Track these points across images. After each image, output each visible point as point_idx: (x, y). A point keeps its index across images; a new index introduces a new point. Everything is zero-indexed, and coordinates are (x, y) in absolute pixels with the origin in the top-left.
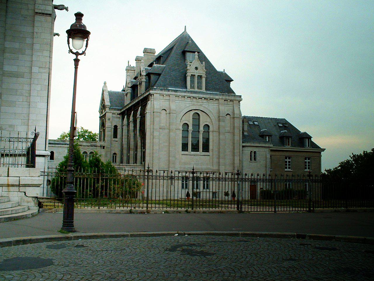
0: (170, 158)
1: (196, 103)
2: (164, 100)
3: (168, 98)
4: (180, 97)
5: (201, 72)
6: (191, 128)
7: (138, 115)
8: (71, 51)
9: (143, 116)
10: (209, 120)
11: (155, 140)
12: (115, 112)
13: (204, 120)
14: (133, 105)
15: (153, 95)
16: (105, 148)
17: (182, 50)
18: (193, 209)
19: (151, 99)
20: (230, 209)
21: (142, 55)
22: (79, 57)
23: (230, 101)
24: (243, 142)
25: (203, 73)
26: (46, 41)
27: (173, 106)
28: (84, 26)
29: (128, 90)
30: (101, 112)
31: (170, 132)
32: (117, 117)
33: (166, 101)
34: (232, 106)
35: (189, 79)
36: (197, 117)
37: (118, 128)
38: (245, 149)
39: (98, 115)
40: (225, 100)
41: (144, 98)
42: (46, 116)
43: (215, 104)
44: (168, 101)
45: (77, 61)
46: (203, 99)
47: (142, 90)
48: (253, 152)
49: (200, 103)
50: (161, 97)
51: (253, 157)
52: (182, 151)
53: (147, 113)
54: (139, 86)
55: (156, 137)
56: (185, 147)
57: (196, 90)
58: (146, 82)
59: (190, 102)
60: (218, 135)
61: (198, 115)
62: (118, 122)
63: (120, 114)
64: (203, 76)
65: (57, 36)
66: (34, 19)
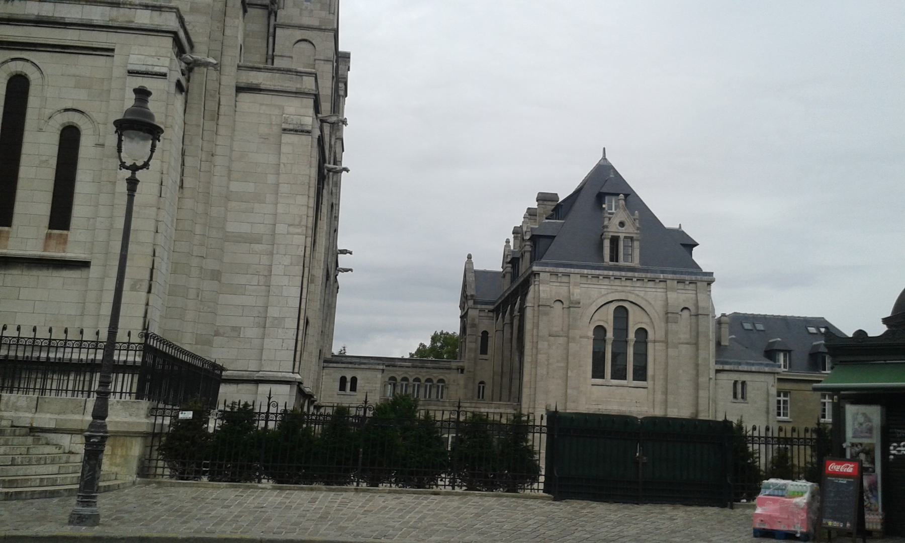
0: (569, 391)
2: (558, 284)
3: (565, 279)
6: (610, 335)
7: (516, 313)
8: (123, 165)
9: (522, 310)
10: (646, 319)
11: (540, 356)
12: (483, 307)
13: (635, 321)
14: (510, 294)
15: (539, 274)
17: (597, 192)
18: (453, 489)
19: (535, 281)
20: (530, 490)
22: (139, 175)
24: (717, 362)
25: (636, 232)
27: (577, 292)
28: (151, 116)
29: (507, 267)
30: (462, 307)
31: (568, 342)
32: (487, 317)
34: (694, 292)
35: (607, 244)
36: (621, 314)
37: (489, 335)
38: (723, 376)
39: (459, 312)
40: (678, 282)
41: (524, 280)
42: (298, 310)
43: (658, 290)
44: (567, 285)
45: (132, 184)
46: (635, 279)
47: (523, 266)
48: (740, 382)
49: (629, 288)
50: (554, 278)
51: (739, 392)
52: (593, 377)
53: (528, 308)
54: (521, 260)
55: (542, 352)
56: (598, 372)
58: (531, 252)
59: (610, 287)
60: (664, 348)
62: (485, 324)
64: (634, 238)
65: (346, 172)
66: (281, 140)
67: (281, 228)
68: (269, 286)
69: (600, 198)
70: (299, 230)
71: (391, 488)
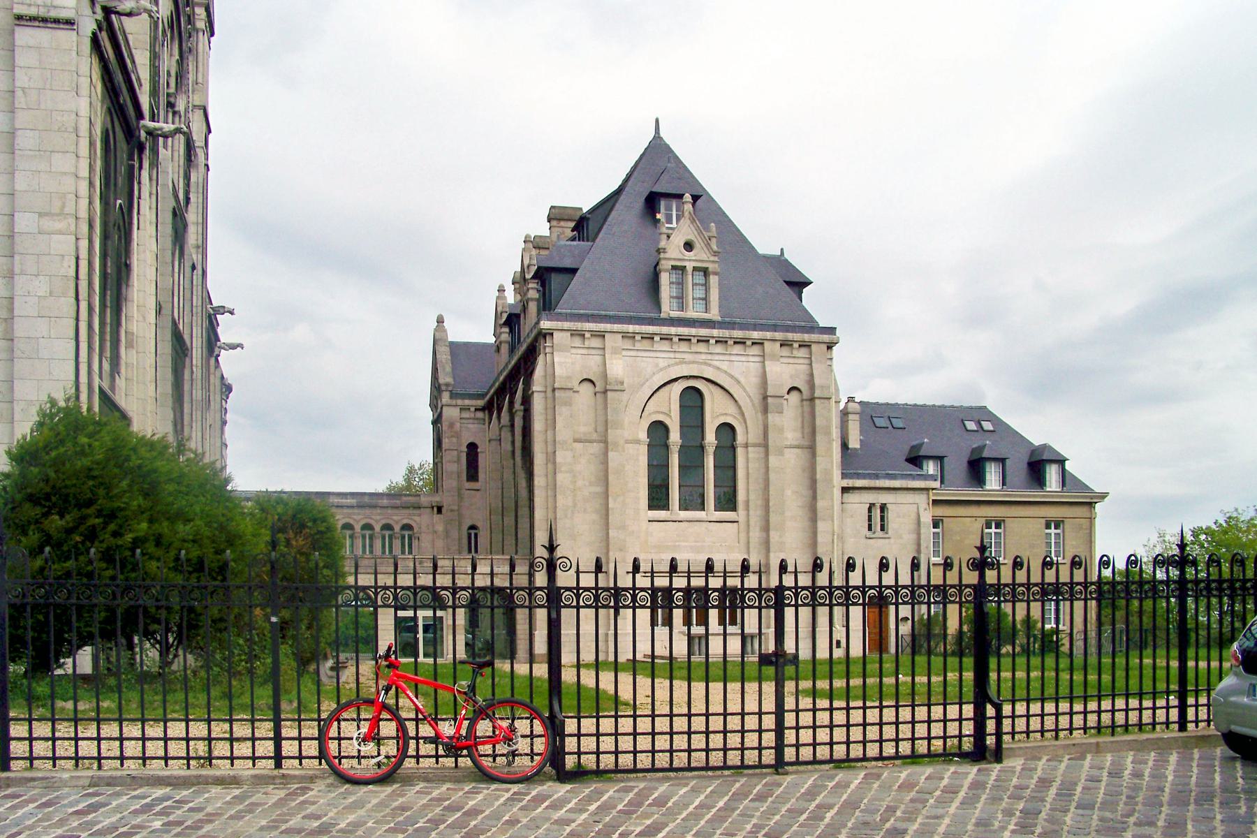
1: (688, 357)
3: (596, 343)
4: (638, 337)
5: (704, 257)
6: (675, 437)
9: (527, 401)
10: (732, 409)
11: (560, 477)
12: (467, 402)
13: (716, 411)
15: (552, 334)
16: (444, 510)
17: (646, 194)
19: (545, 347)
21: (543, 229)
23: (800, 346)
24: (844, 476)
25: (712, 258)
26: (59, 118)
27: (618, 367)
33: (593, 352)
34: (807, 361)
35: (664, 278)
36: (693, 401)
38: (852, 497)
39: (429, 415)
40: (781, 345)
46: (712, 341)
48: (878, 505)
49: (703, 357)
50: (577, 342)
51: (878, 519)
52: (651, 507)
53: (535, 394)
54: (522, 316)
56: (658, 498)
57: (691, 314)
58: (538, 300)
59: (672, 355)
60: (762, 455)
61: (698, 396)
62: (472, 430)
63: (483, 409)
64: (710, 270)
67: (24, 222)
68: (12, 340)
69: (652, 202)
70: (58, 225)
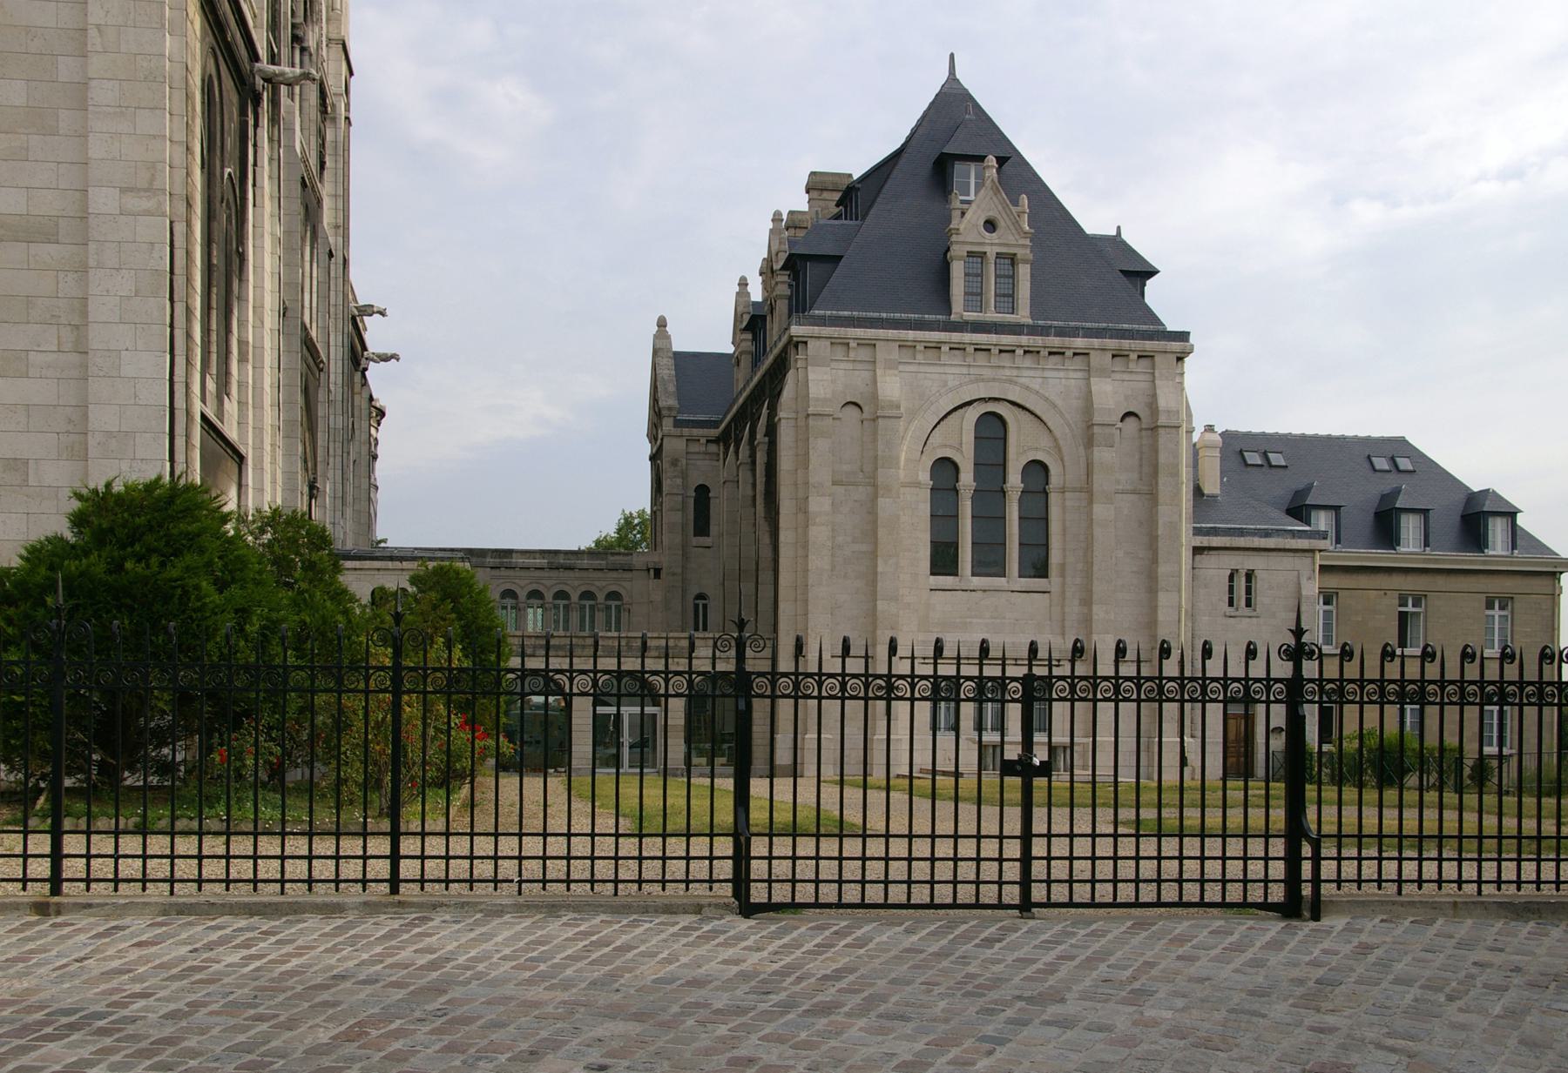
1: (987, 373)
2: (850, 366)
3: (864, 354)
4: (920, 347)
5: (1011, 239)
6: (967, 478)
9: (772, 431)
10: (1045, 441)
12: (696, 432)
13: (1022, 446)
15: (806, 343)
16: (663, 574)
19: (796, 360)
23: (1139, 357)
24: (1198, 532)
25: (1022, 242)
26: (145, 64)
27: (892, 386)
30: (653, 437)
32: (706, 453)
33: (859, 366)
34: (1148, 377)
35: (957, 270)
36: (992, 430)
37: (710, 495)
38: (1206, 560)
39: (646, 449)
40: (1114, 356)
41: (775, 360)
43: (1072, 375)
46: (1020, 352)
48: (1243, 573)
49: (1007, 372)
50: (840, 352)
51: (1240, 593)
53: (783, 421)
54: (768, 318)
56: (943, 560)
57: (991, 315)
58: (790, 298)
59: (965, 371)
61: (1000, 424)
63: (716, 441)
64: (1019, 256)
67: (103, 200)
68: (87, 353)
70: (146, 204)
71: (173, 899)
